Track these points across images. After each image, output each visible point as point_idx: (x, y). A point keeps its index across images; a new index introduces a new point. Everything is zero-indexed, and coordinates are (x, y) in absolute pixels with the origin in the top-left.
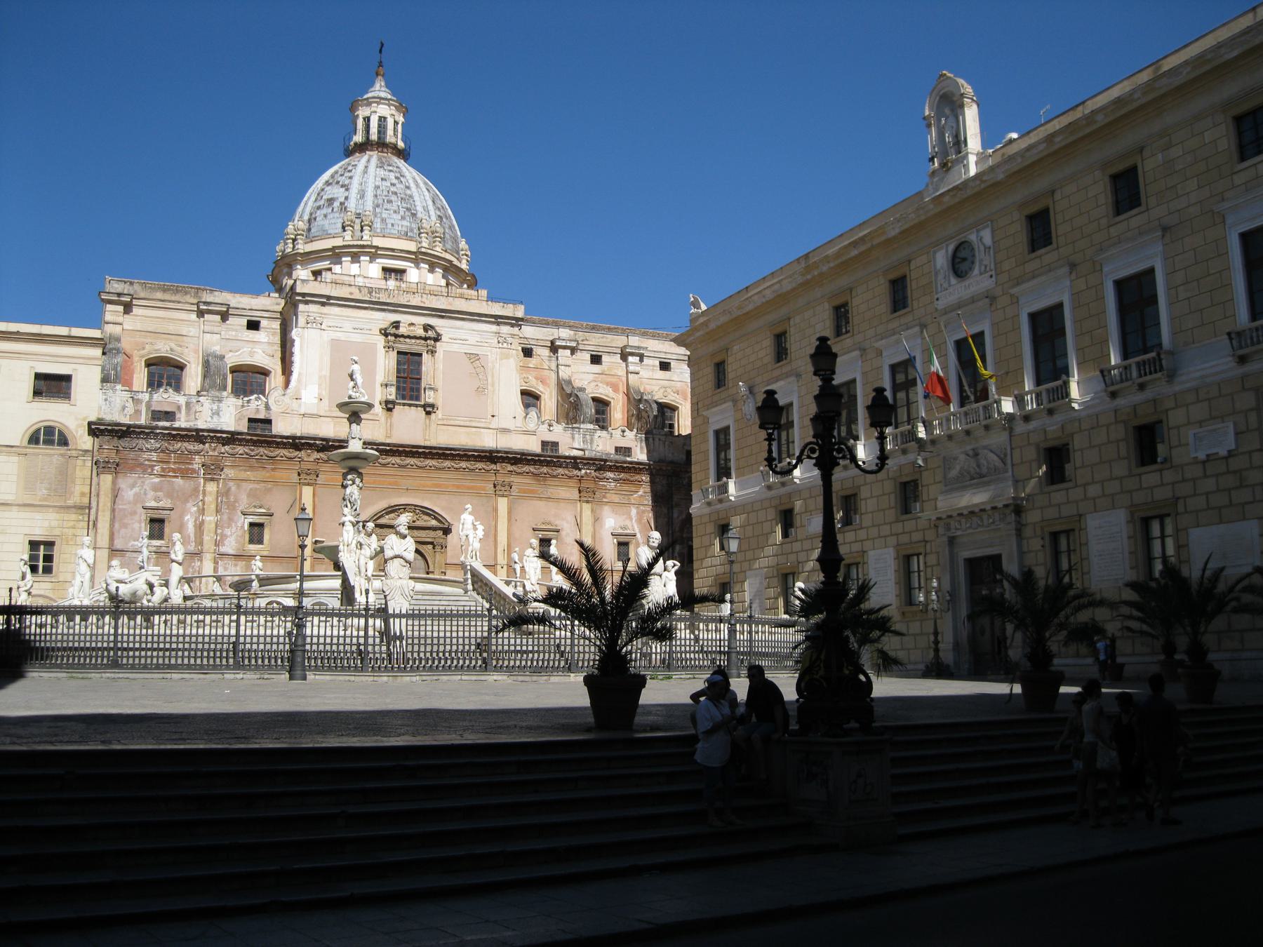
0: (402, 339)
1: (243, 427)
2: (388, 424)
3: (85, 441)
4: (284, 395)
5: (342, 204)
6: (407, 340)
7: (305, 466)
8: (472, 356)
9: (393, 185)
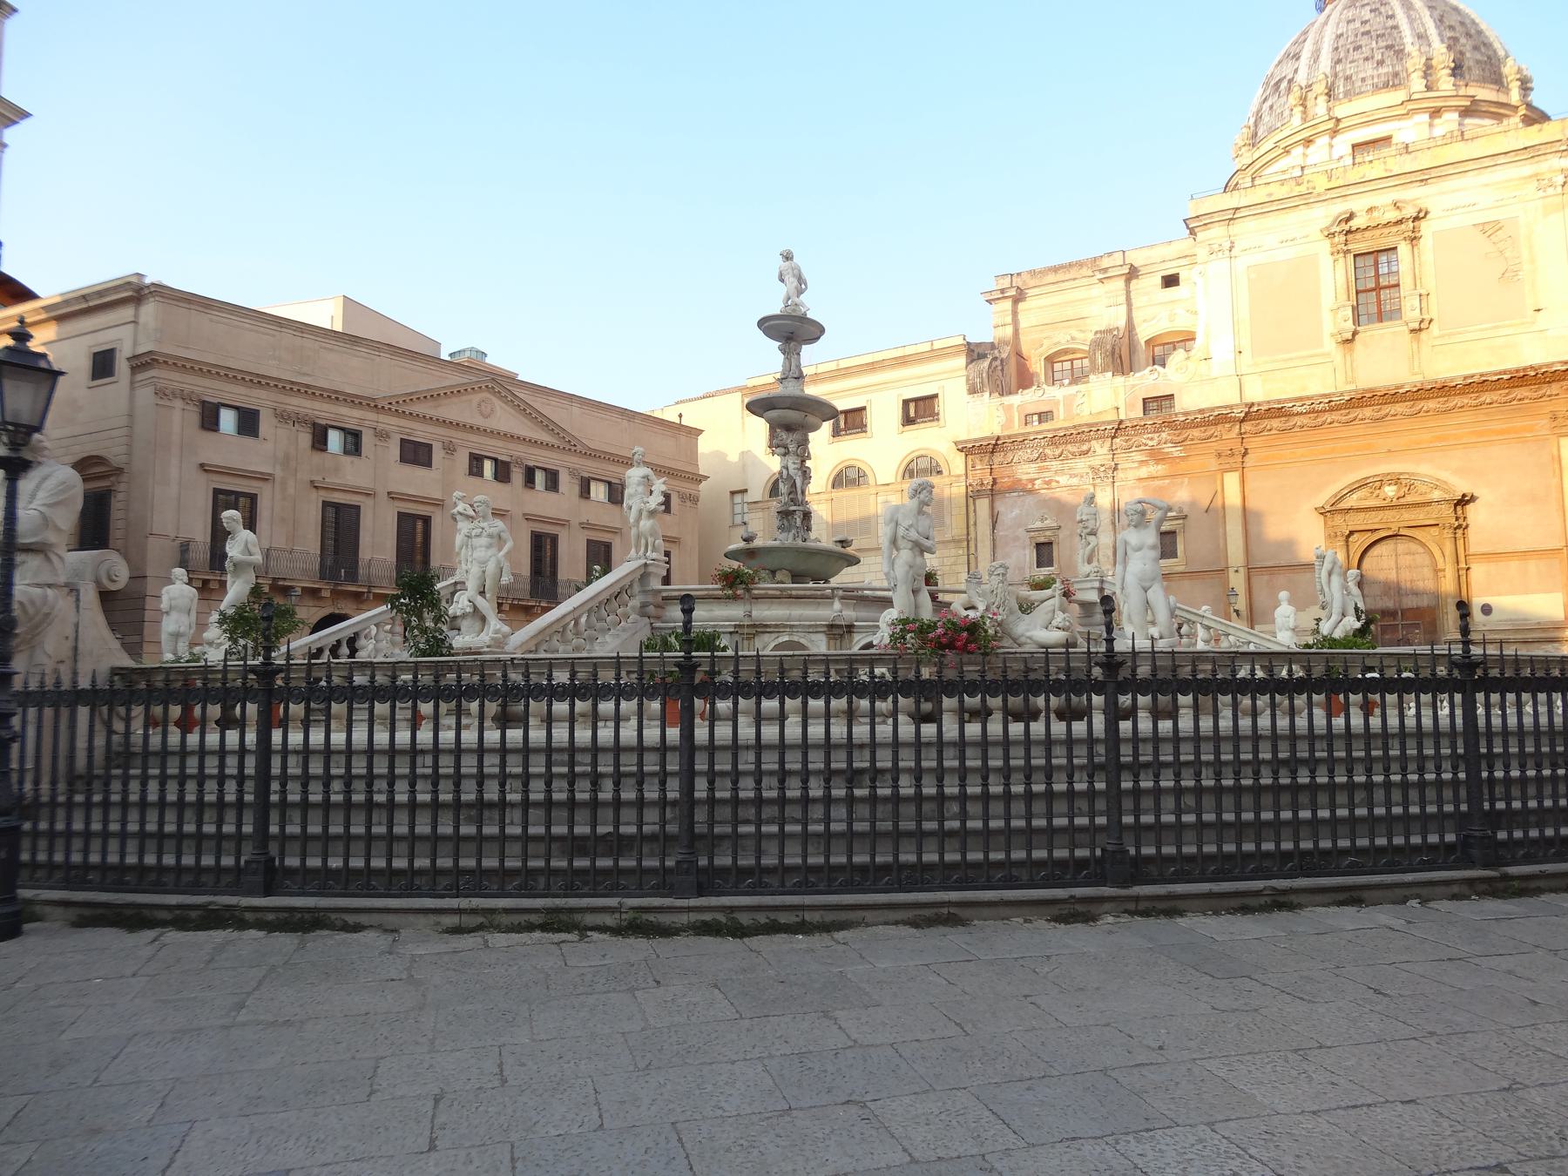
0: (1358, 236)
1: (1138, 412)
2: (1348, 363)
3: (957, 463)
4: (1188, 358)
5: (1290, 81)
6: (1367, 234)
7: (1224, 447)
8: (1487, 228)
9: (1364, 23)
